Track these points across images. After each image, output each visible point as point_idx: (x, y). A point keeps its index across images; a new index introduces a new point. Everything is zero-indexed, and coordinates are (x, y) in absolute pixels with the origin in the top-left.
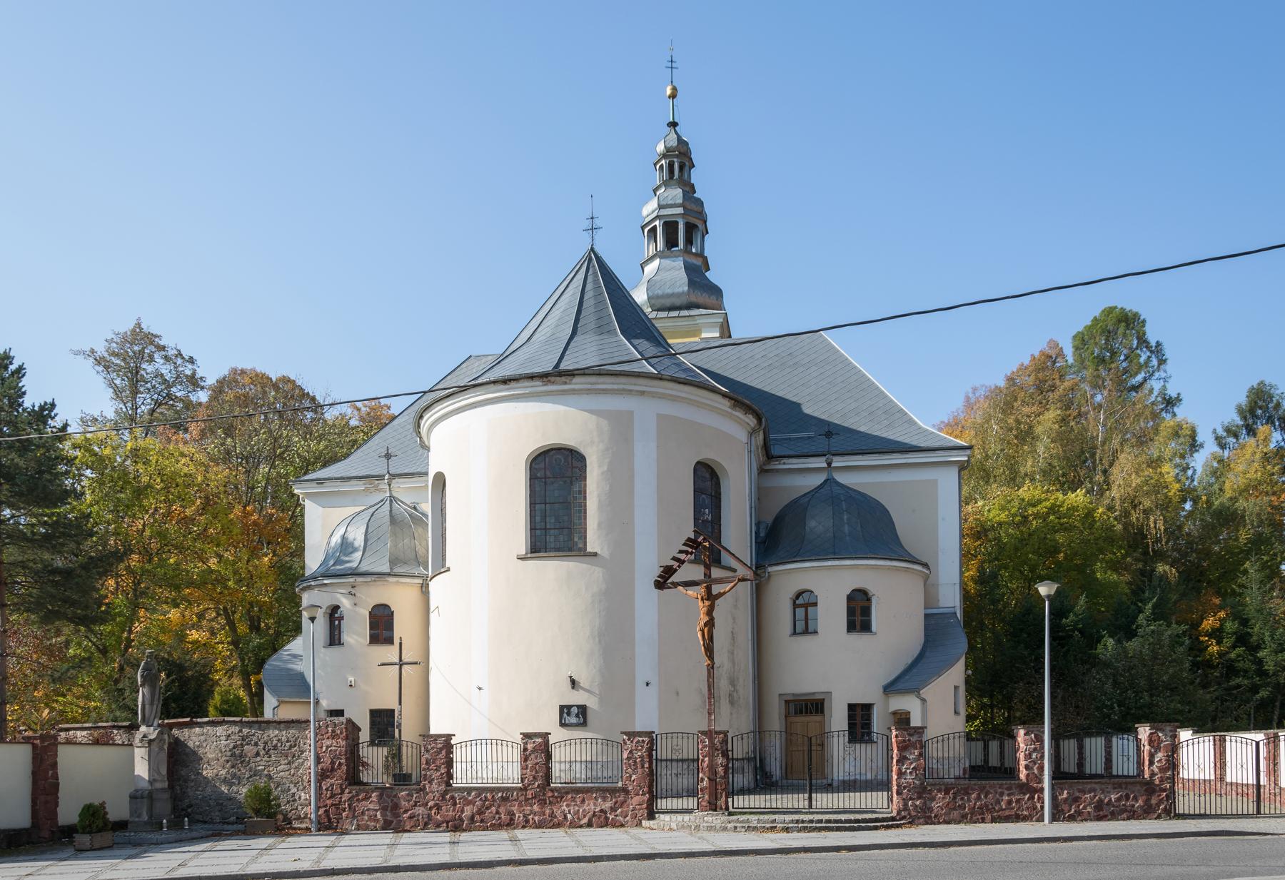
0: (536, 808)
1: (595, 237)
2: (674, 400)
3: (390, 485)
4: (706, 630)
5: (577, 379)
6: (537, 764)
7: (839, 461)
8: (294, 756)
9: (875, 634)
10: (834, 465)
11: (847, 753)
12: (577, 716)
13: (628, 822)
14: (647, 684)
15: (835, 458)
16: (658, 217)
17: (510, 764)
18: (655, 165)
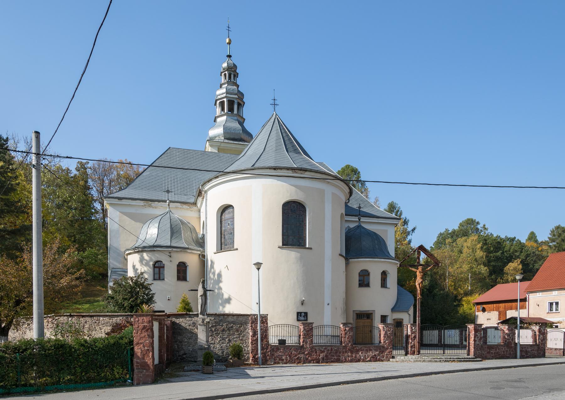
0: (349, 354)
1: (276, 108)
2: (337, 187)
3: (169, 205)
5: (307, 173)
6: (350, 336)
7: (363, 219)
8: (241, 331)
9: (389, 288)
12: (304, 317)
13: (384, 359)
15: (362, 218)
17: (274, 337)
18: (221, 73)
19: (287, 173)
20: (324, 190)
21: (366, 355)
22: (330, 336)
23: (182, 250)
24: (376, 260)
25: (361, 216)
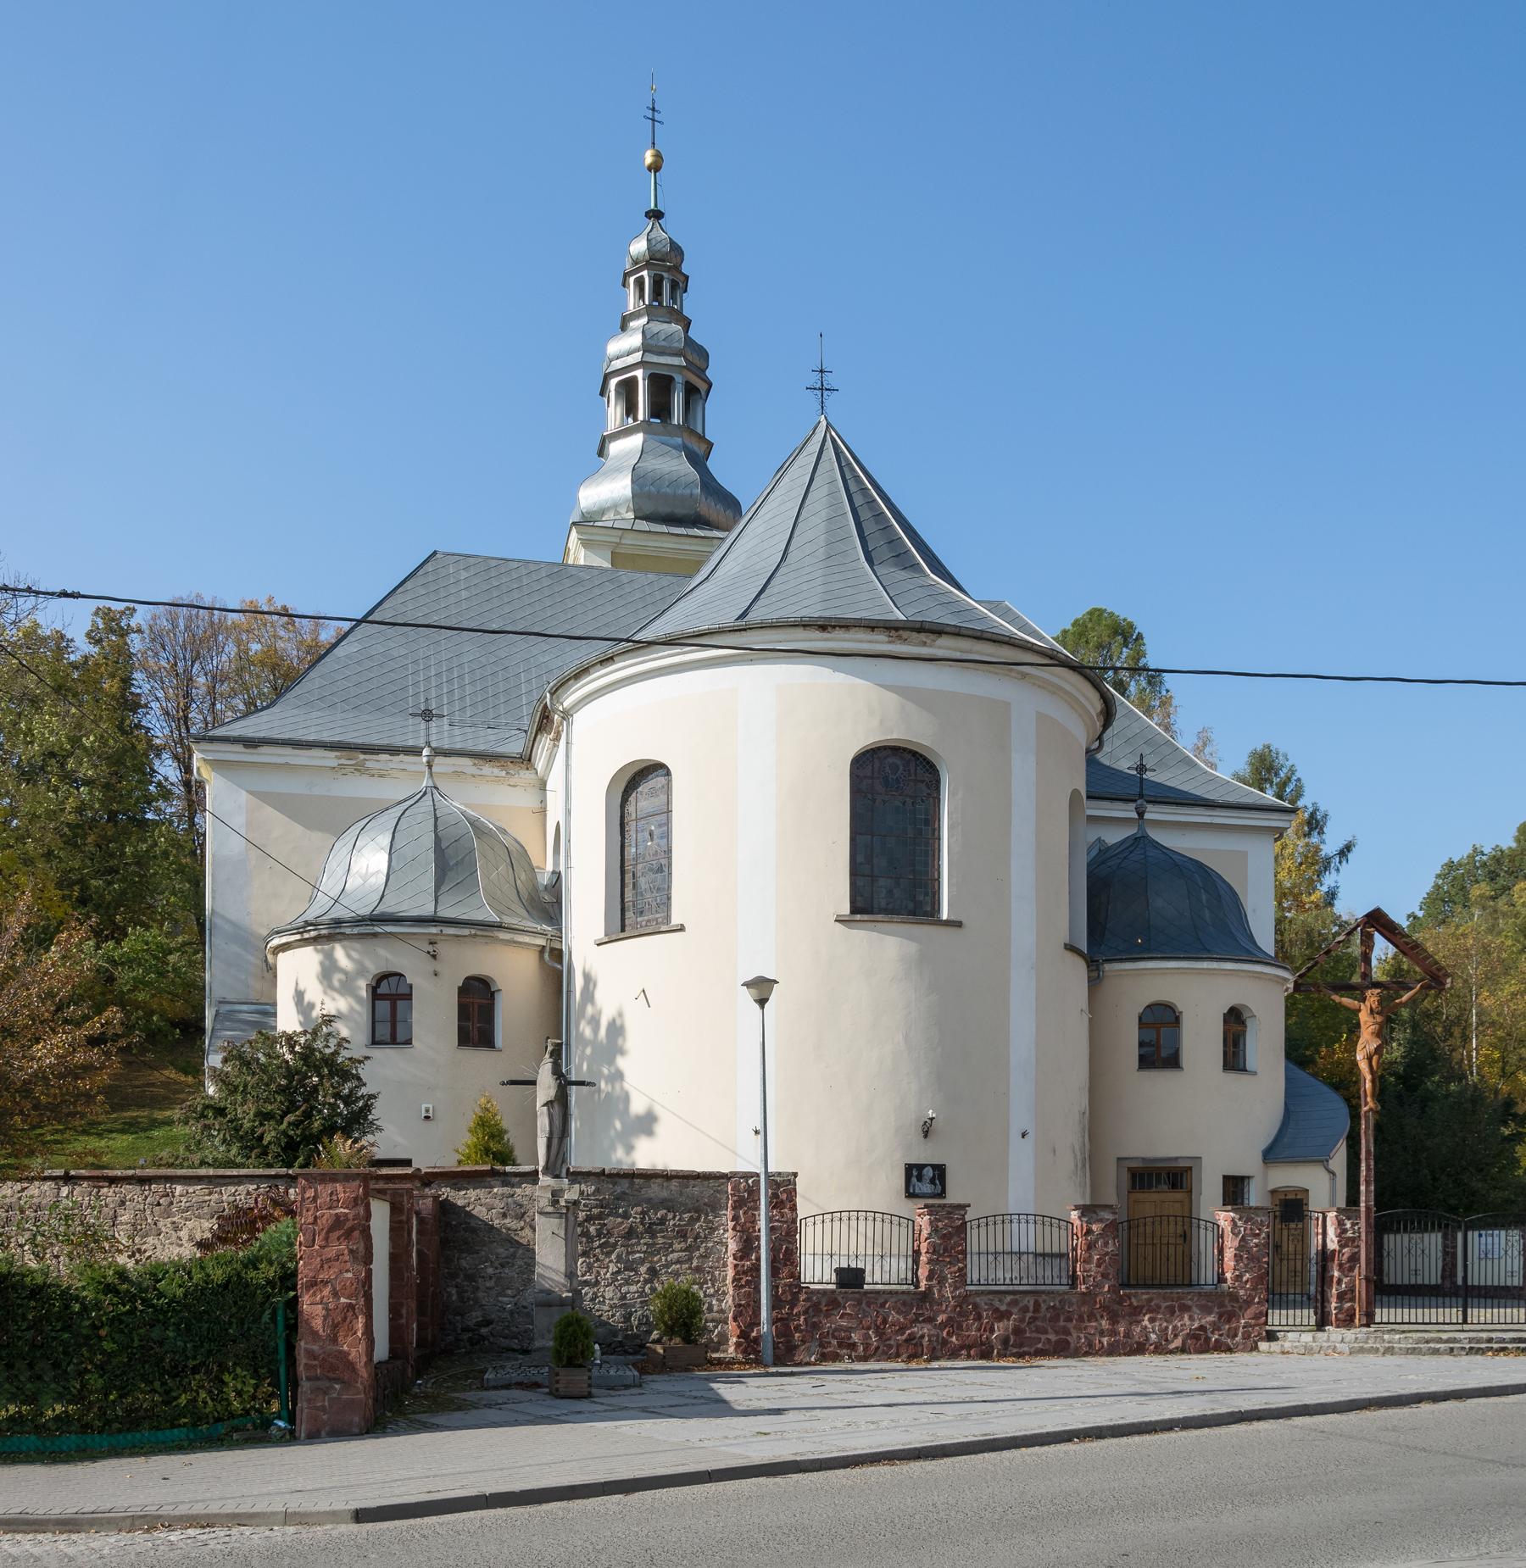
0: (1105, 1324)
1: (826, 403)
2: (1054, 693)
3: (430, 767)
4: (1375, 1058)
5: (944, 641)
6: (1107, 1254)
7: (1154, 813)
8: (697, 1237)
9: (1255, 1073)
10: (1147, 816)
11: (1510, 1244)
12: (932, 1181)
13: (1237, 1345)
14: (1023, 1135)
15: (1150, 807)
18: (626, 275)
19: (870, 642)
20: (1007, 705)
21: (1167, 1328)
22: (1031, 1256)
23: (479, 933)
24: (1205, 965)
25: (1149, 802)
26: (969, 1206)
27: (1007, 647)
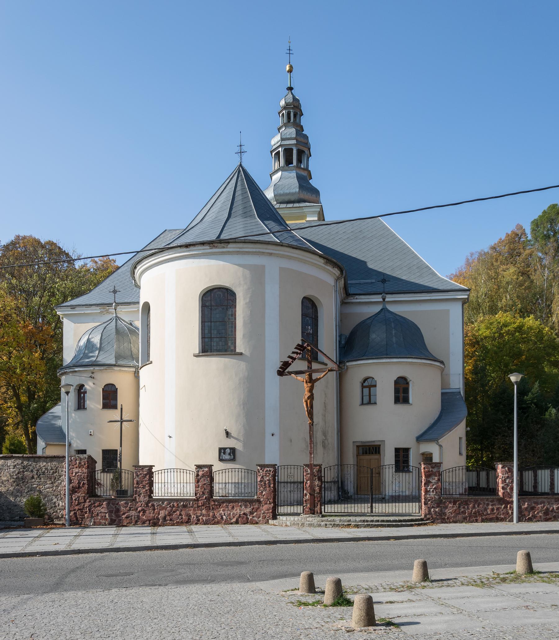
0: (204, 512)
1: (242, 158)
2: (291, 259)
3: (116, 310)
4: (309, 401)
5: (231, 245)
6: (205, 484)
7: (389, 298)
9: (412, 405)
10: (387, 300)
11: (394, 478)
12: (230, 454)
13: (260, 521)
14: (273, 435)
15: (388, 296)
16: (280, 146)
18: (279, 113)
19: (203, 249)
20: (263, 267)
21: (230, 513)
22: (230, 485)
23: (107, 368)
24: (384, 360)
25: (387, 294)
26: (213, 466)
27: (259, 244)
